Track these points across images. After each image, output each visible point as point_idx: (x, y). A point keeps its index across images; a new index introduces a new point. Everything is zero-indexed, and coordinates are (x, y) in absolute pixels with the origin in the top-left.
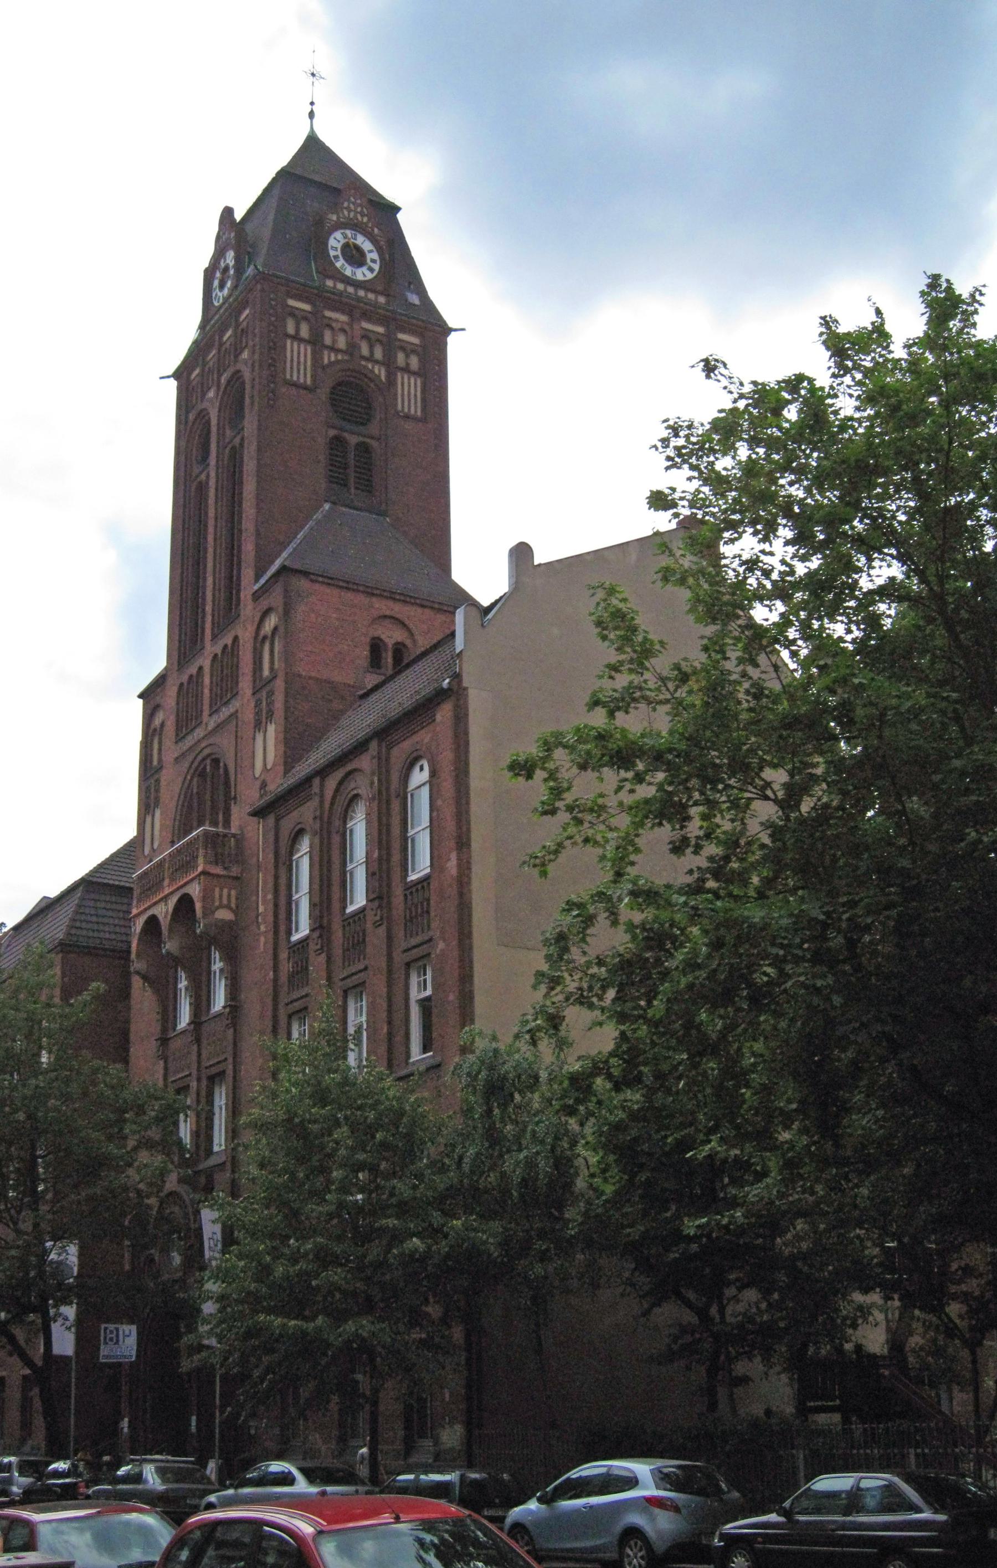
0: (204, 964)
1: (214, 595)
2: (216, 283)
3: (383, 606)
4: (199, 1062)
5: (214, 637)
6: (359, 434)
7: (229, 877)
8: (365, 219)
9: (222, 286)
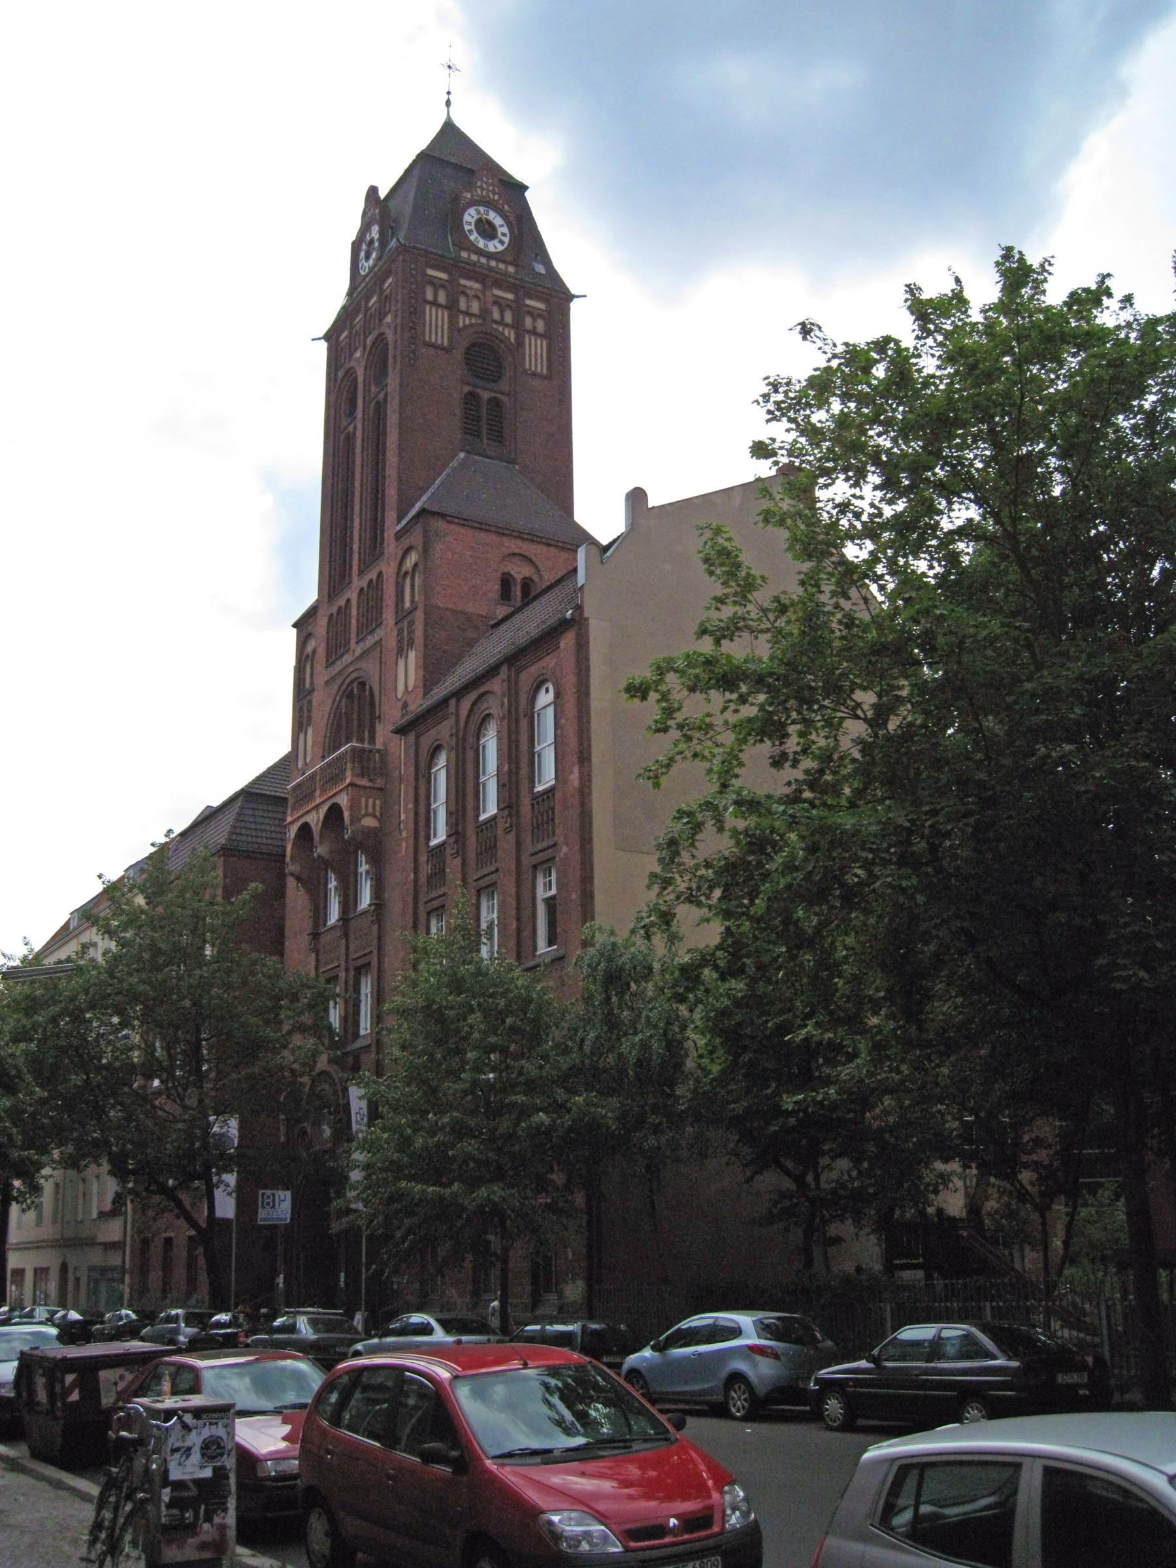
0: (352, 867)
1: (360, 535)
2: (362, 254)
3: (512, 545)
4: (347, 955)
5: (361, 572)
6: (491, 390)
7: (374, 788)
8: (496, 197)
9: (367, 257)
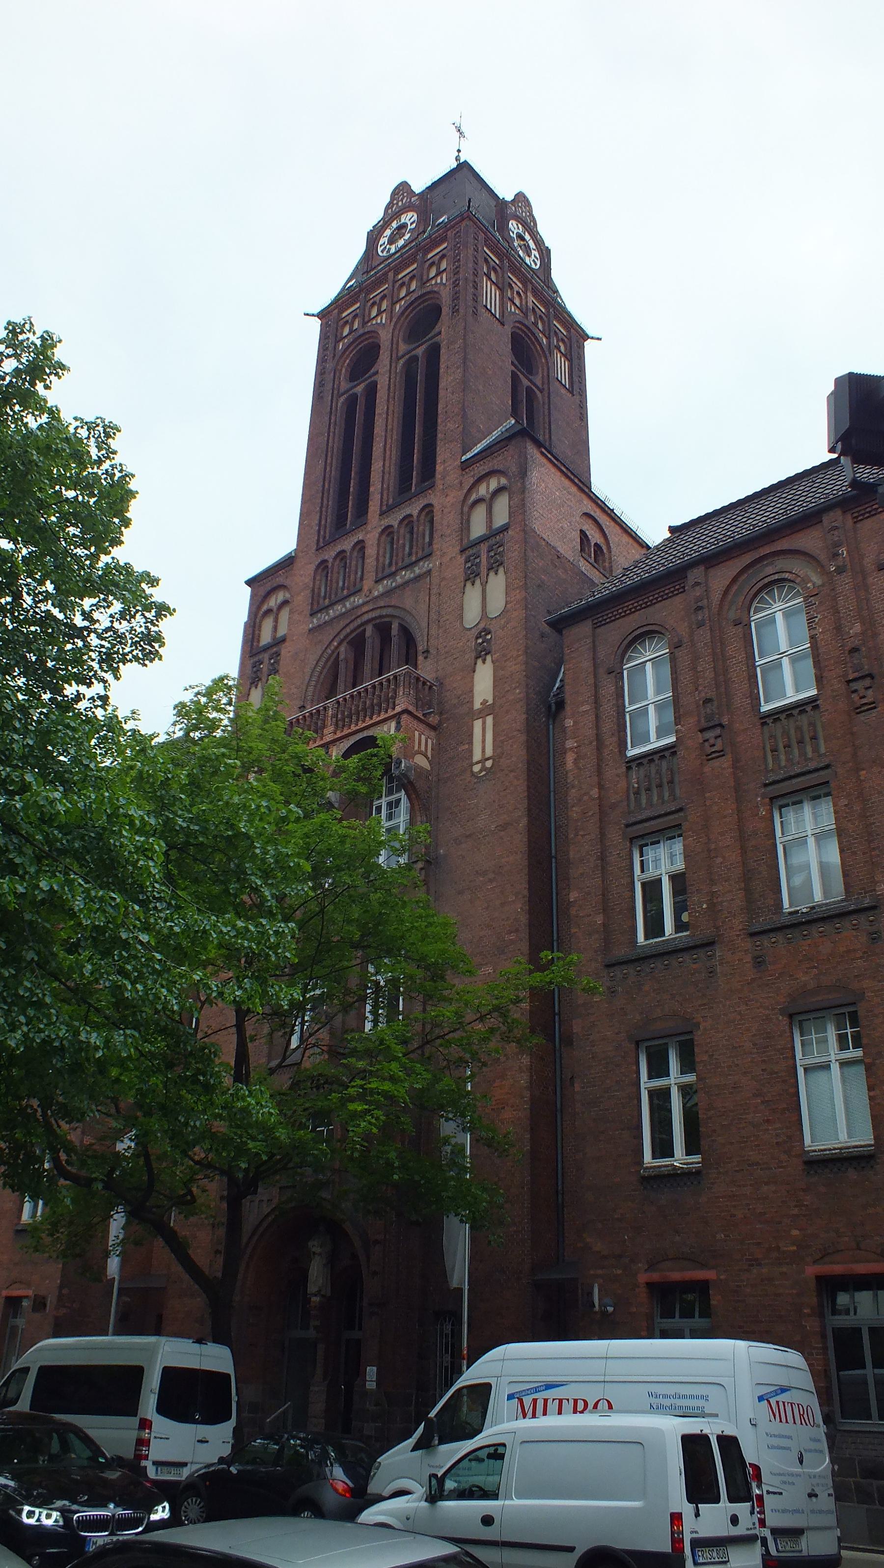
2: (384, 240)
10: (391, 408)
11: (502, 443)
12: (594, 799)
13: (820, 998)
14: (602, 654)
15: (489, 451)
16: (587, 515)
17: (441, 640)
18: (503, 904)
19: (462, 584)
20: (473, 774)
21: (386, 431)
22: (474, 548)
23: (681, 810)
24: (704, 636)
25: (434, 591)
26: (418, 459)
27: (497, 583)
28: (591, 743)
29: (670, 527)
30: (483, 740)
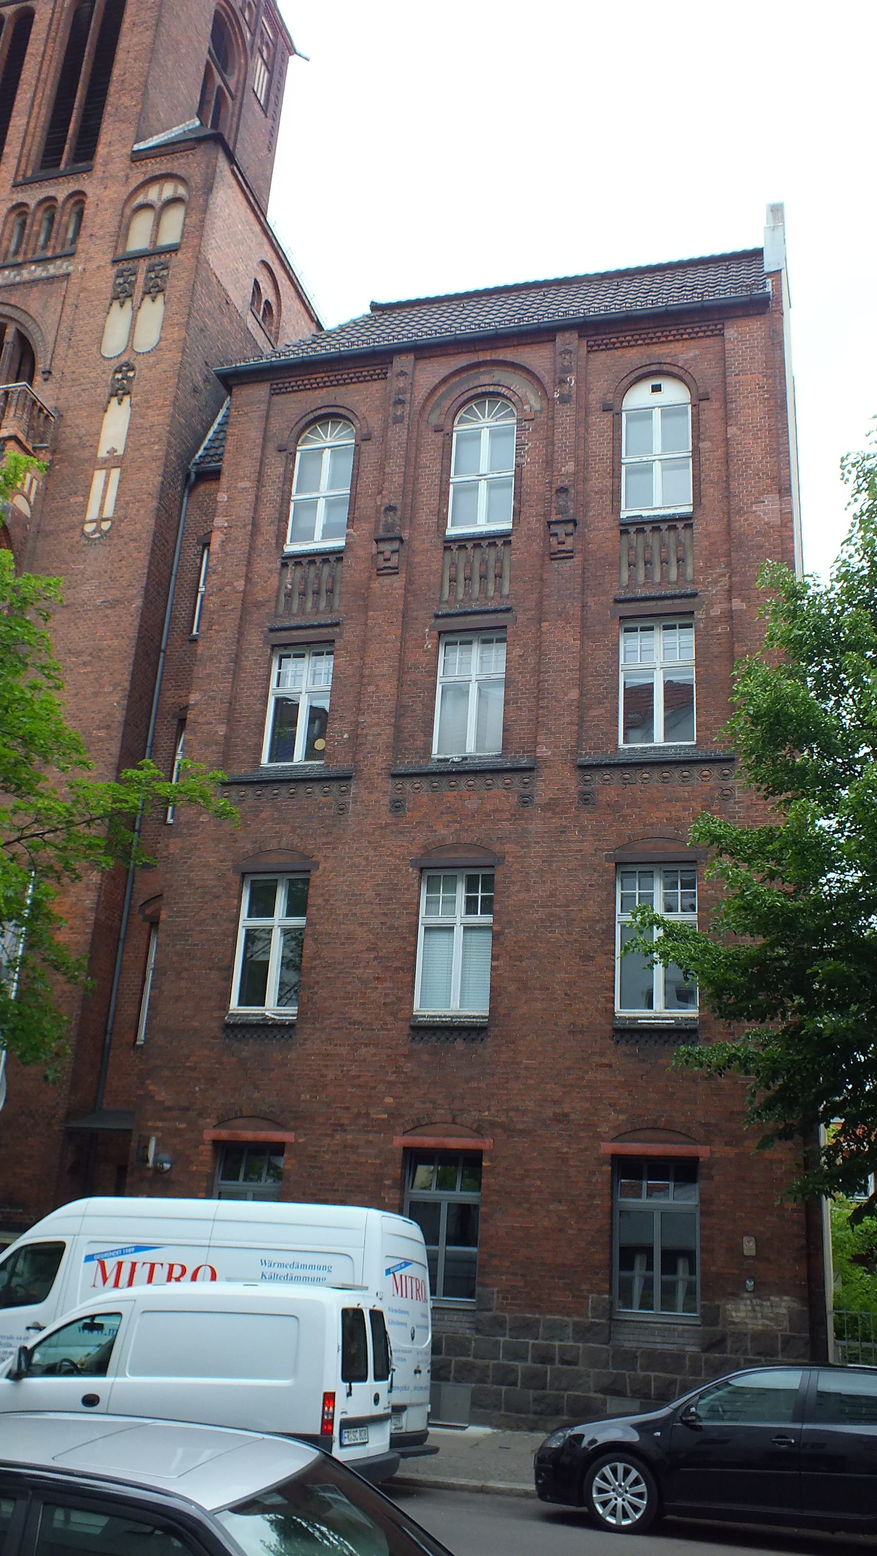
10: (49, 52)
11: (189, 143)
12: (236, 592)
13: (456, 855)
14: (276, 425)
15: (171, 147)
16: (265, 264)
17: (69, 363)
18: (96, 694)
19: (108, 302)
20: (83, 533)
21: (38, 80)
22: (131, 262)
23: (337, 624)
24: (398, 435)
25: (69, 301)
26: (75, 130)
27: (153, 313)
28: (245, 526)
29: (372, 302)
30: (102, 496)
